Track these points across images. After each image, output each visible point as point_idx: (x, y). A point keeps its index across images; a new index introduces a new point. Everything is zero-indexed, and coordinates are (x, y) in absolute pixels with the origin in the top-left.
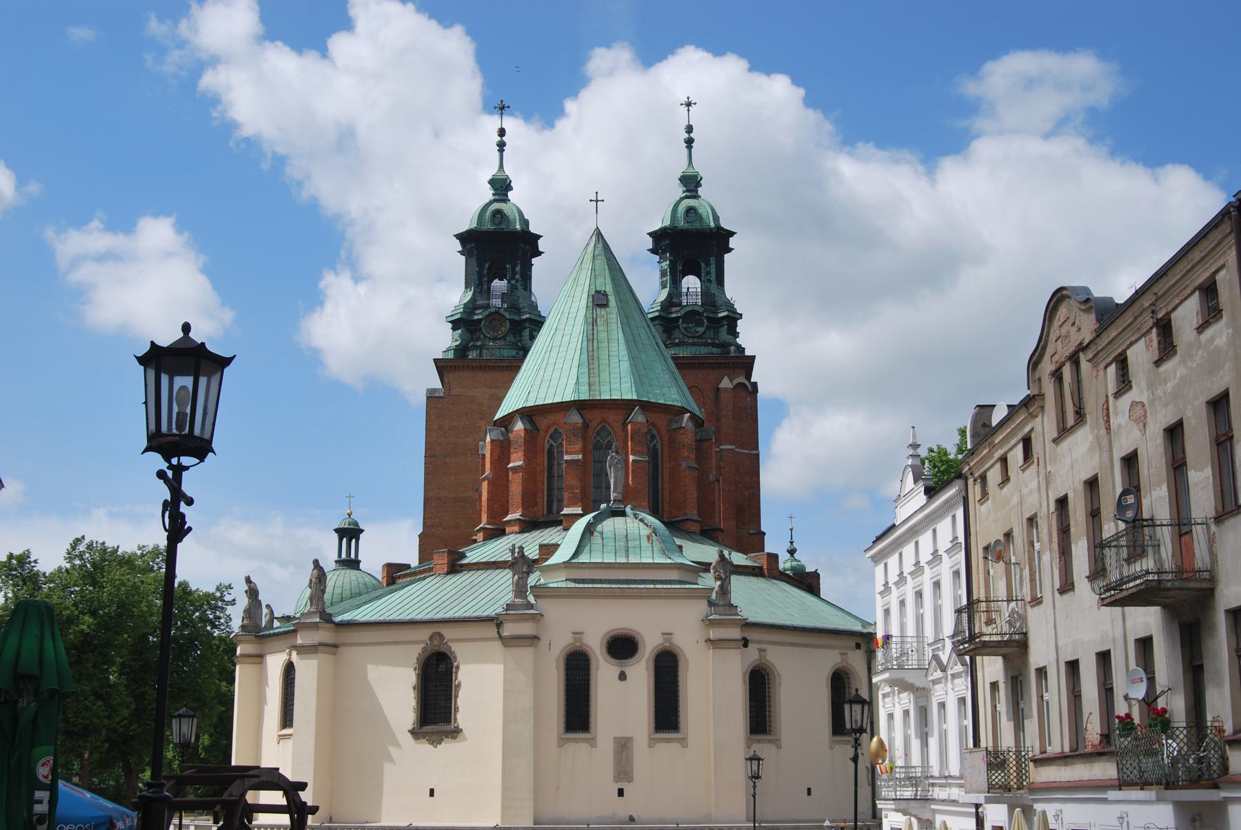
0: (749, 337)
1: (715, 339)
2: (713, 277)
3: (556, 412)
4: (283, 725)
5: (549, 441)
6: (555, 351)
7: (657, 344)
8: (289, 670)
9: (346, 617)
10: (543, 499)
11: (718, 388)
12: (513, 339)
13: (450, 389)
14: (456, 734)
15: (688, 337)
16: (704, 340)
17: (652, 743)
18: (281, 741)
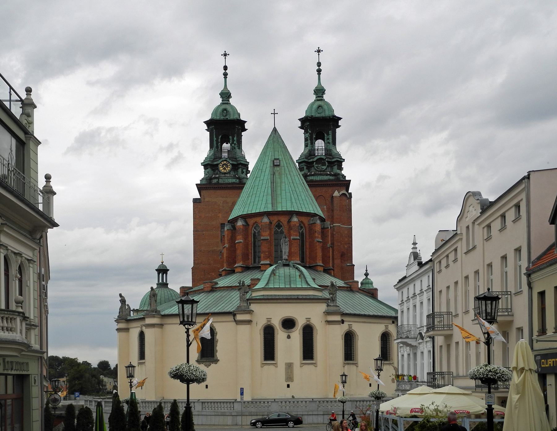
0: (347, 171)
1: (331, 172)
2: (331, 141)
3: (257, 217)
4: (140, 359)
5: (254, 230)
6: (256, 188)
7: (303, 183)
8: (142, 336)
9: (167, 312)
10: (251, 257)
11: (333, 196)
12: (234, 173)
13: (204, 198)
14: (216, 362)
15: (318, 171)
16: (326, 173)
17: (302, 365)
18: (140, 365)
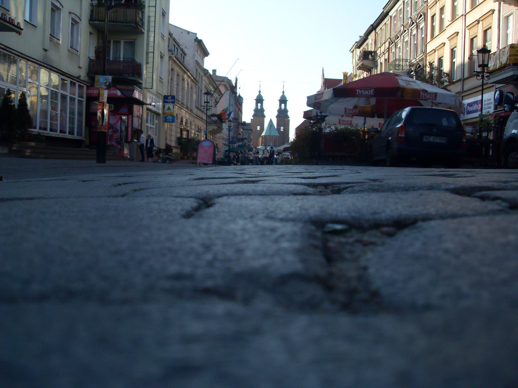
0: (289, 114)
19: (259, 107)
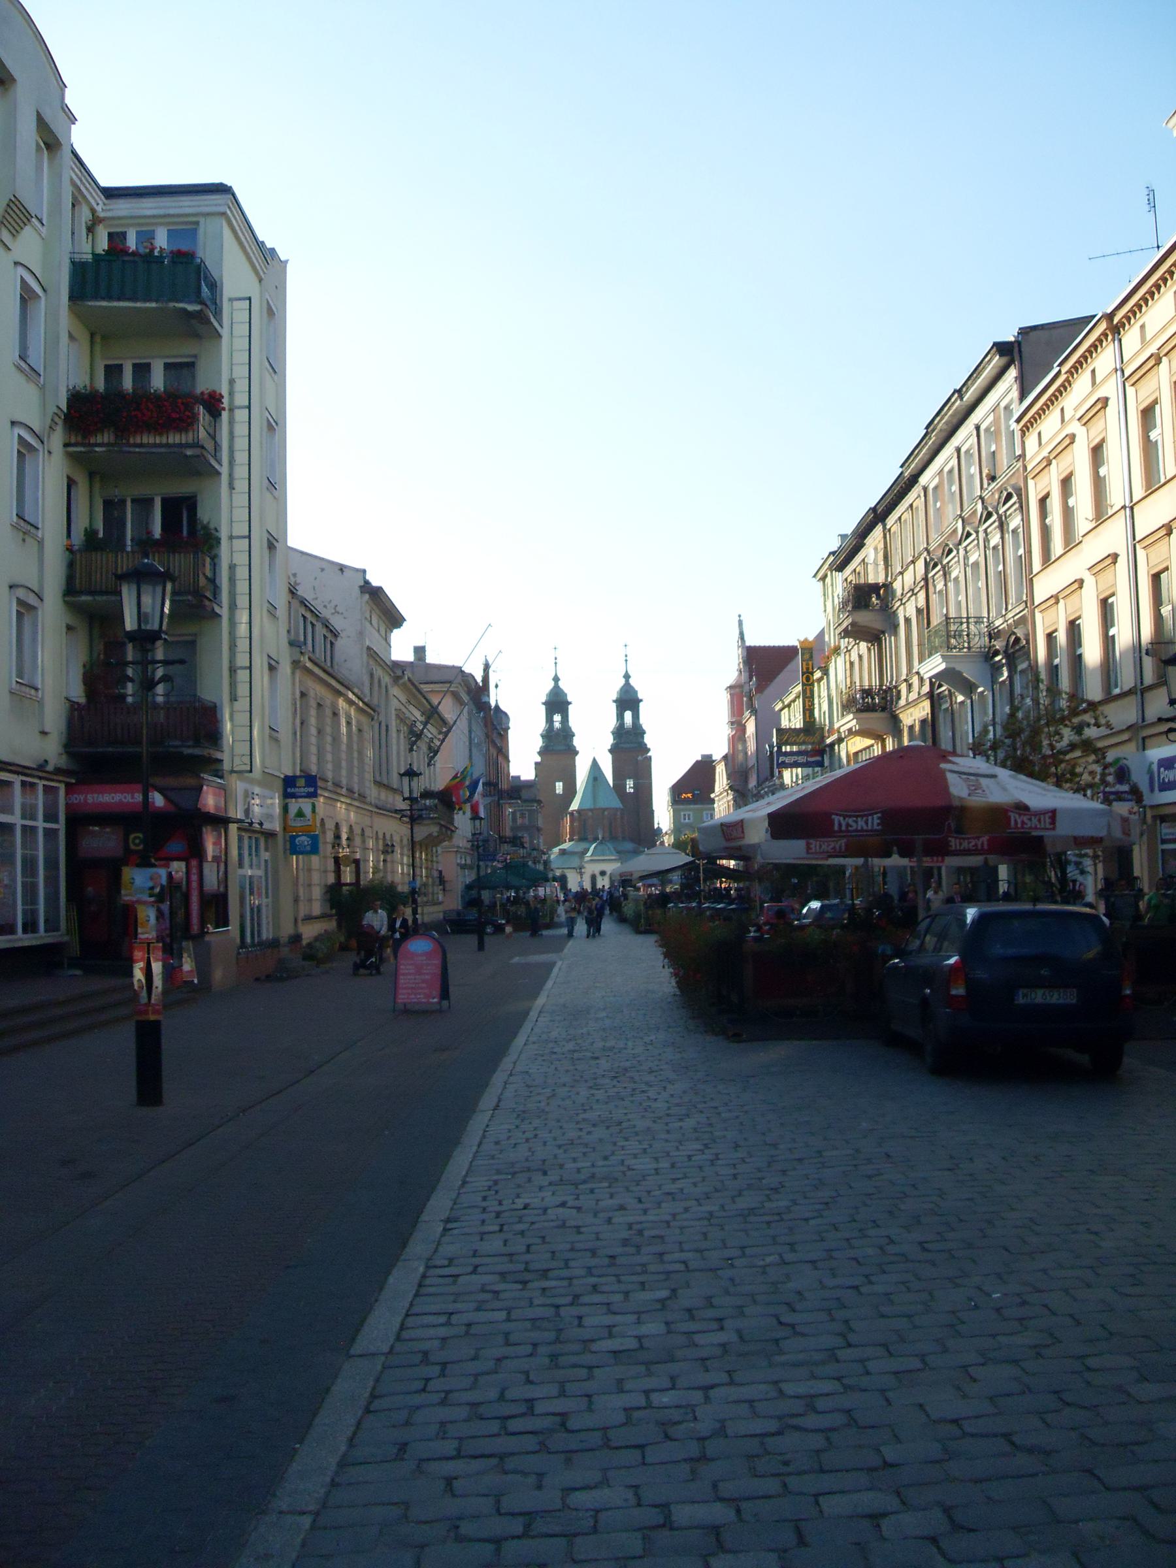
0: (648, 740)
19: (557, 725)
